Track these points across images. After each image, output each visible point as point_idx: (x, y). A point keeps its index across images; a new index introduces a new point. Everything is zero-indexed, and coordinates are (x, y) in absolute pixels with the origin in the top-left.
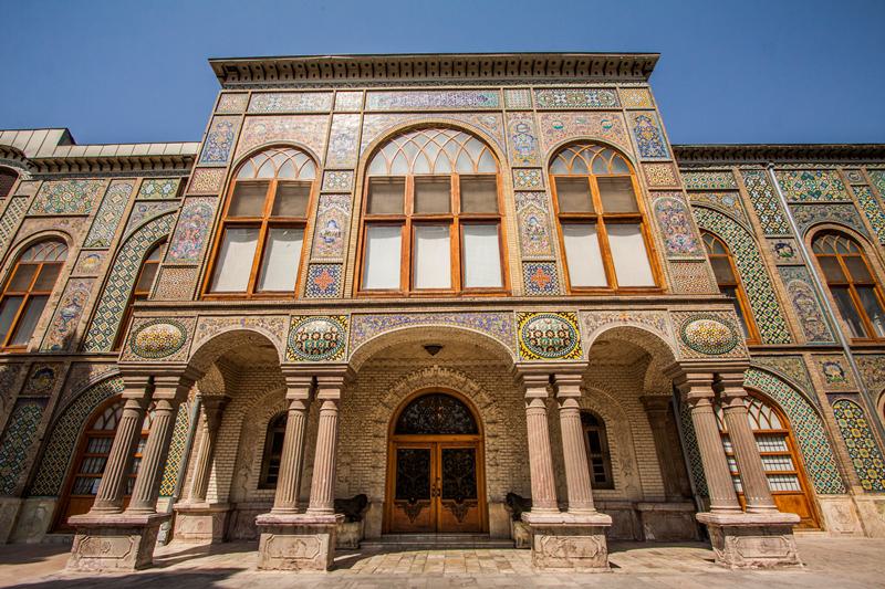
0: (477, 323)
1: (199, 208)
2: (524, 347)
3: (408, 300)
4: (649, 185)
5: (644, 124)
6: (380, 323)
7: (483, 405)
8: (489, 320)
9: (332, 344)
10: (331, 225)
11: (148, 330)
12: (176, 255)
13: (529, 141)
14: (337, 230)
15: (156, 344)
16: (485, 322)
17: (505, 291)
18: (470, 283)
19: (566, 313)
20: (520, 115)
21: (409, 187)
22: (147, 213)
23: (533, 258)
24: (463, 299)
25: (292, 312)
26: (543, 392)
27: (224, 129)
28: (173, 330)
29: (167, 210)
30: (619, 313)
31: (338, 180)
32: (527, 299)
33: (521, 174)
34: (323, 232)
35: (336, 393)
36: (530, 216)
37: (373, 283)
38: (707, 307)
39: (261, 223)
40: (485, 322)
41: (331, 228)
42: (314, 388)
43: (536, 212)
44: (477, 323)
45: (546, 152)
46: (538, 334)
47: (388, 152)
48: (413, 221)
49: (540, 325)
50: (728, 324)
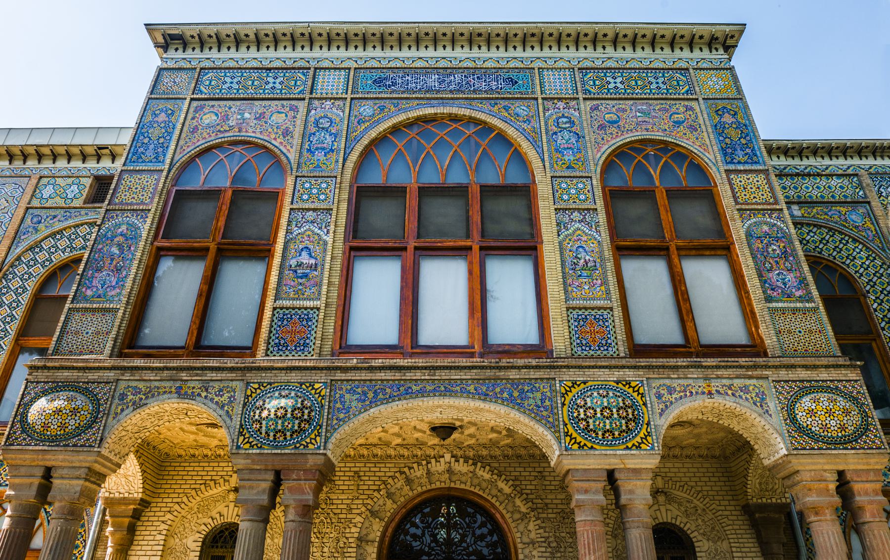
0: (505, 395)
1: (124, 228)
2: (571, 431)
4: (737, 203)
5: (728, 119)
6: (371, 395)
7: (517, 516)
8: (522, 392)
10: (304, 253)
12: (89, 293)
13: (573, 140)
14: (313, 261)
16: (516, 394)
19: (628, 383)
20: (561, 105)
21: (412, 200)
22: (41, 226)
23: (581, 303)
27: (162, 117)
29: (71, 222)
30: (701, 383)
31: (315, 191)
32: (573, 362)
33: (564, 186)
34: (293, 262)
36: (578, 244)
39: (207, 249)
40: (516, 394)
41: (305, 258)
43: (584, 238)
44: (505, 395)
46: (590, 413)
47: (385, 157)
48: (416, 248)
50: (854, 400)
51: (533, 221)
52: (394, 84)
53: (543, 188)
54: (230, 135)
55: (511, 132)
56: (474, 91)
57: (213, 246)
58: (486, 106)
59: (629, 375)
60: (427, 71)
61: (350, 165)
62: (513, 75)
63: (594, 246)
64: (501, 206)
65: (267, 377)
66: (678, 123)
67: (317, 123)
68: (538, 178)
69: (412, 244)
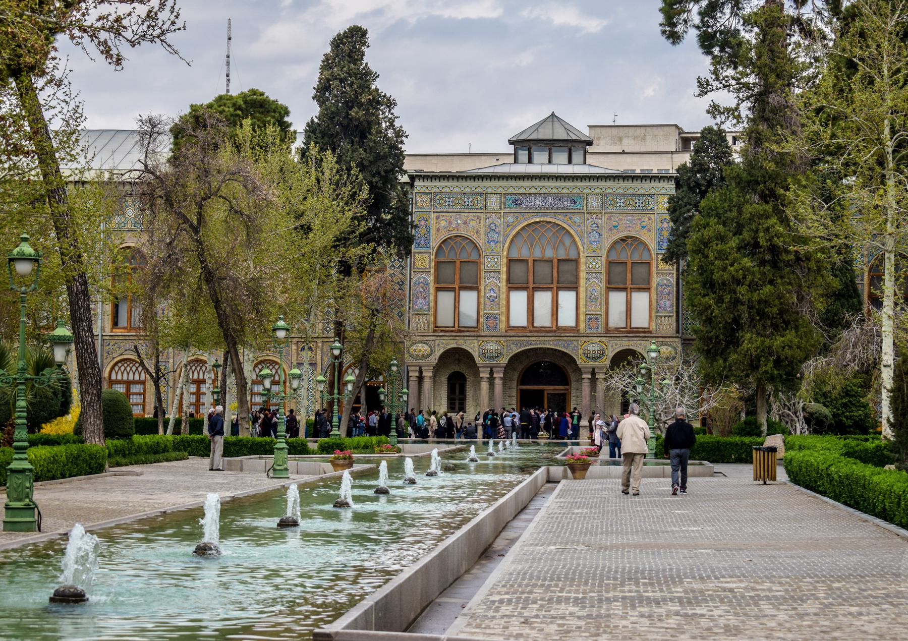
3: (531, 328)
9: (499, 355)
11: (414, 347)
15: (420, 353)
17: (575, 329)
18: (561, 324)
20: (594, 216)
24: (556, 330)
25: (479, 339)
26: (589, 376)
28: (426, 347)
34: (488, 295)
35: (502, 375)
37: (513, 323)
38: (668, 340)
41: (493, 294)
42: (491, 373)
45: (607, 245)
49: (591, 348)
51: (577, 277)
52: (522, 203)
53: (582, 262)
54: (454, 233)
55: (572, 231)
56: (558, 208)
57: (457, 287)
58: (562, 217)
59: (603, 339)
60: (535, 195)
61: (506, 249)
62: (575, 198)
63: (598, 288)
64: (566, 267)
65: (485, 339)
66: (643, 227)
67: (490, 227)
68: (581, 256)
69: (531, 286)
